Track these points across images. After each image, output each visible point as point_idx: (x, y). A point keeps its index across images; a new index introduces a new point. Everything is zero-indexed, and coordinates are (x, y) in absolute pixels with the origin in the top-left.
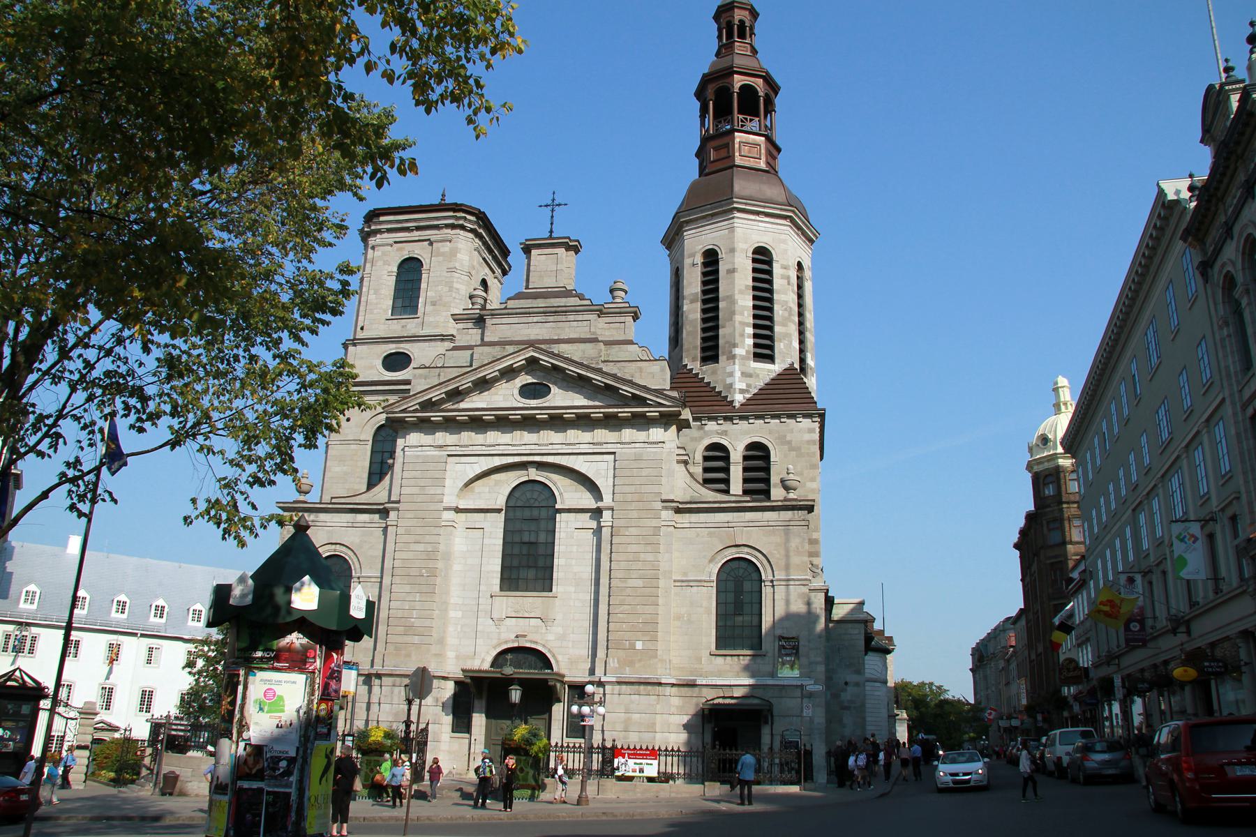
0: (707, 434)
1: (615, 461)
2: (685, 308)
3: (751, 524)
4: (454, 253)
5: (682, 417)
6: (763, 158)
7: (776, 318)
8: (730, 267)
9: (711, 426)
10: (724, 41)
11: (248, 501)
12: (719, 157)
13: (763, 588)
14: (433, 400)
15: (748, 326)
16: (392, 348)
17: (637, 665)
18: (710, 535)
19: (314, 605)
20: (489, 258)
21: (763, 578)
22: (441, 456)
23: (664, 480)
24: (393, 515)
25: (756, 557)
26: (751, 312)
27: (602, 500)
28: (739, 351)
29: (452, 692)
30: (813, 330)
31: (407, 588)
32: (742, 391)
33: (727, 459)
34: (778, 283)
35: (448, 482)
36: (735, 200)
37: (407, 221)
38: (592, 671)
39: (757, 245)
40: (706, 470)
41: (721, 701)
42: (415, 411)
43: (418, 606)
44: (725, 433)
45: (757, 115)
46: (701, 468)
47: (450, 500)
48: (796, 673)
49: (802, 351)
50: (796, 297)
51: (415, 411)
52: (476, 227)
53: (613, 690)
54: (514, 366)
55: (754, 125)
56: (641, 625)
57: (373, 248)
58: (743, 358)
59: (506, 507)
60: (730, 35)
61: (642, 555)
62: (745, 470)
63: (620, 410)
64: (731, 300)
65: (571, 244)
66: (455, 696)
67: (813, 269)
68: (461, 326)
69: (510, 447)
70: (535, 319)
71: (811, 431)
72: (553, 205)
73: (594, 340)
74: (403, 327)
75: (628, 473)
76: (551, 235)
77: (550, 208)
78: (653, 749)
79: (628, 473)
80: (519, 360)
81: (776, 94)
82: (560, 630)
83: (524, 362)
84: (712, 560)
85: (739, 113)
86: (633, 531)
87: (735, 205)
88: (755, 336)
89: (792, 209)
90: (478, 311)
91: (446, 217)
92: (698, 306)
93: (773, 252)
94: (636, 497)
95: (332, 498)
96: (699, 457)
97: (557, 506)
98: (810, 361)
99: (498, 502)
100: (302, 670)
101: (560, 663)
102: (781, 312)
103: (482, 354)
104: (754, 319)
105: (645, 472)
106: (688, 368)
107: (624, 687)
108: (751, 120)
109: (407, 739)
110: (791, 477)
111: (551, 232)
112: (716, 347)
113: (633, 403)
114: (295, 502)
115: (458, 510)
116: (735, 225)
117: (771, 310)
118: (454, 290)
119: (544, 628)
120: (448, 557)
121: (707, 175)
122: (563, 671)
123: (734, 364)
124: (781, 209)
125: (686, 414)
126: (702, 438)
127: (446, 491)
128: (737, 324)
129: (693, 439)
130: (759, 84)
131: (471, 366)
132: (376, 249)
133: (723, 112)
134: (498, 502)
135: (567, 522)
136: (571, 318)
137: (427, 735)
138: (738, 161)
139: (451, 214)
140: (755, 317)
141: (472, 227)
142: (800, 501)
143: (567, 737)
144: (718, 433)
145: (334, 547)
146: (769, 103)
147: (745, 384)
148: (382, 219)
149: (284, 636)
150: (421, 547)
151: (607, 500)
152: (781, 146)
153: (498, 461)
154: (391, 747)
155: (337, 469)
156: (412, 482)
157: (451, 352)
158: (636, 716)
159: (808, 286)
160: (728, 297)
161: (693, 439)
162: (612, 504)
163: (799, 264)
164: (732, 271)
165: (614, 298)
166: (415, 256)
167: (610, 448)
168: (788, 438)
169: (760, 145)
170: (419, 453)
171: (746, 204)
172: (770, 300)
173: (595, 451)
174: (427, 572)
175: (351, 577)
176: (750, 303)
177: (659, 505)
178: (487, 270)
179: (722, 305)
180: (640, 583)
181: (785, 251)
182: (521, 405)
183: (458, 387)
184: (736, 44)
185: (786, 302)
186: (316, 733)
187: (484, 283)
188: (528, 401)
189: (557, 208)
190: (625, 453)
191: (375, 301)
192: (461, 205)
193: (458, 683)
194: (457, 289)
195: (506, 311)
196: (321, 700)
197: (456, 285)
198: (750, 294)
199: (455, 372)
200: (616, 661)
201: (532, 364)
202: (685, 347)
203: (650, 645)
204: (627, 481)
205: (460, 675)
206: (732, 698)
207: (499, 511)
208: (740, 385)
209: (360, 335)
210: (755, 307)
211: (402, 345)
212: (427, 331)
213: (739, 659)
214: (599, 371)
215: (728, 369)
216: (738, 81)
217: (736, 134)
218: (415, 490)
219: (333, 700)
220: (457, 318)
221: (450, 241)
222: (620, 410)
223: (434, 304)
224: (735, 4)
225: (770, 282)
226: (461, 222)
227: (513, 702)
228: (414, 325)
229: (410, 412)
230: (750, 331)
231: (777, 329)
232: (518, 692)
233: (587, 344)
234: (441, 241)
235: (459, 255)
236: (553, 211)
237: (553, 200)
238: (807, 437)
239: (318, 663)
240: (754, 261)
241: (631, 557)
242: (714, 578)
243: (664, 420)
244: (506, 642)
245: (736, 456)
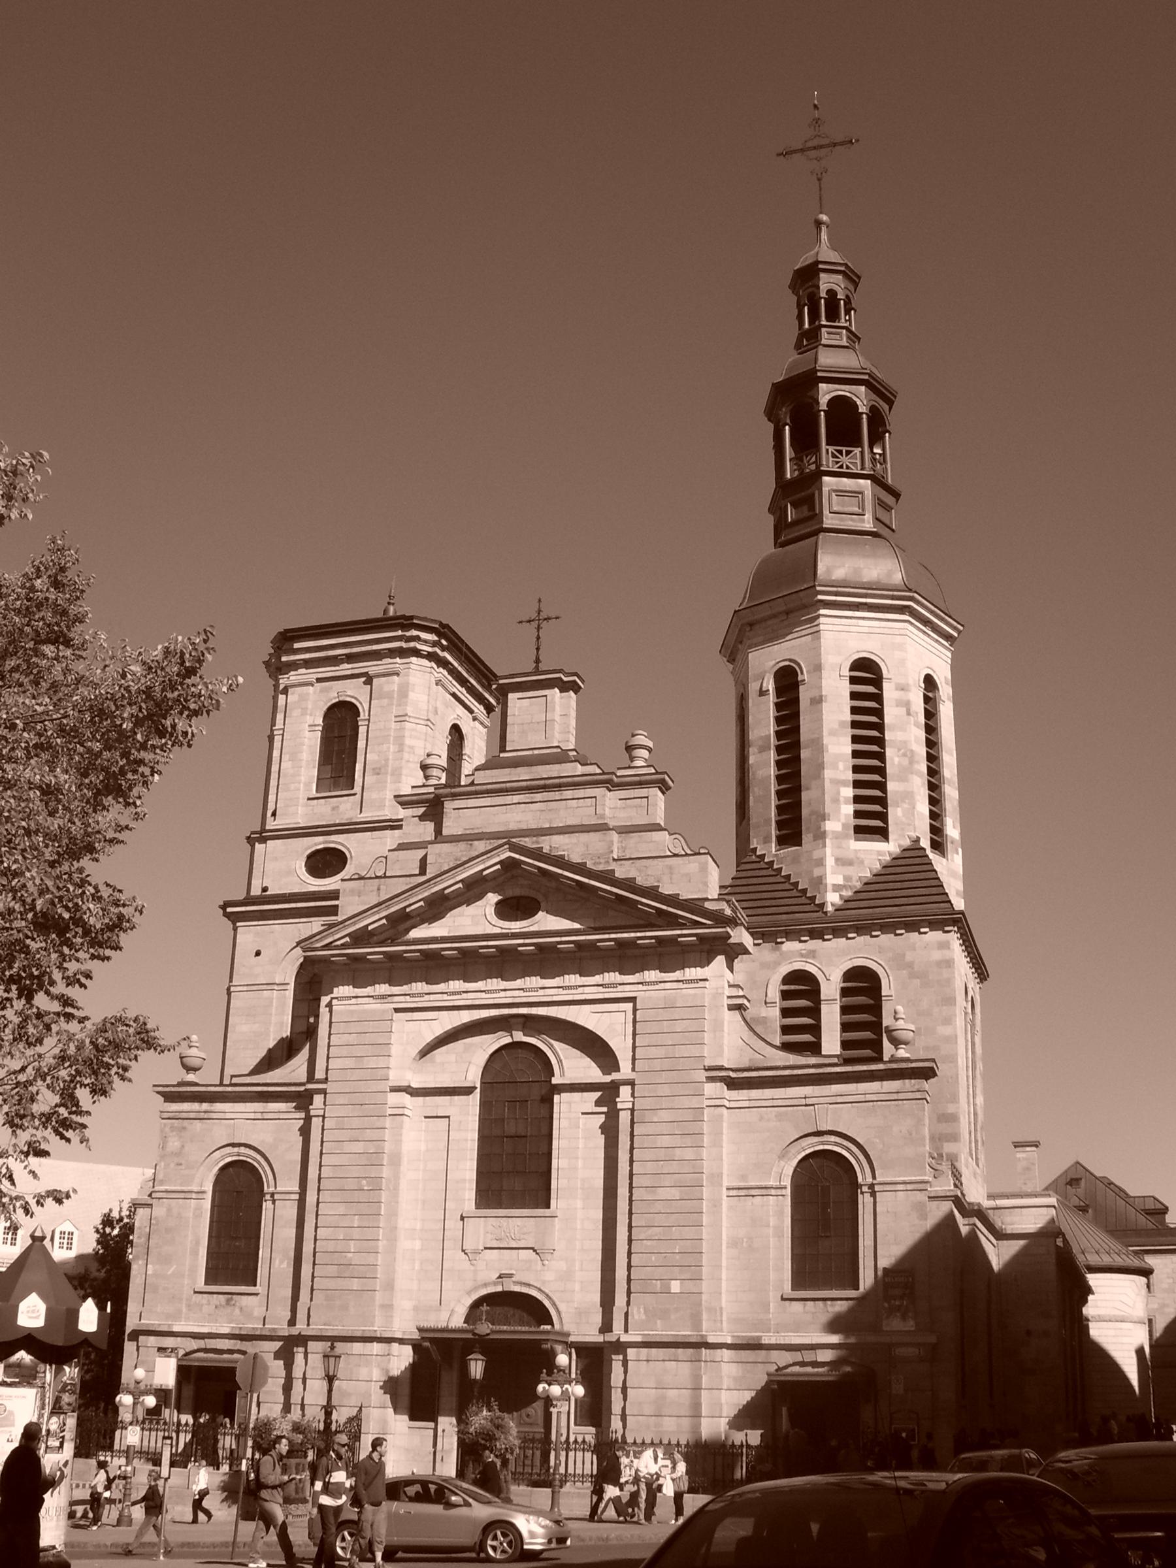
0: (785, 957)
1: (635, 1010)
2: (752, 759)
3: (840, 1099)
4: (404, 692)
5: (732, 941)
6: (869, 516)
7: (890, 770)
8: (814, 693)
9: (790, 946)
10: (807, 326)
11: (28, 1169)
12: (801, 516)
13: (860, 1196)
14: (370, 928)
16: (318, 843)
17: (673, 1317)
18: (778, 1116)
19: (39, 1322)
20: (461, 692)
21: (860, 1180)
22: (384, 1011)
23: (707, 1037)
24: (318, 1100)
25: (848, 1150)
26: (851, 762)
27: (617, 1069)
28: (831, 826)
29: (411, 1361)
30: (956, 779)
31: (341, 1209)
32: (837, 888)
33: (818, 992)
34: (891, 713)
35: (395, 1050)
36: (818, 588)
37: (333, 647)
38: (606, 1327)
40: (786, 1012)
41: (797, 1369)
42: (344, 946)
43: (356, 1233)
44: (812, 954)
45: (858, 443)
46: (778, 1009)
47: (399, 1076)
48: (910, 1325)
49: (934, 816)
50: (922, 734)
51: (344, 946)
52: (437, 650)
53: (638, 1354)
54: (485, 873)
55: (853, 459)
56: (677, 1257)
57: (285, 691)
58: (837, 836)
59: (482, 1083)
60: (814, 315)
61: (678, 1153)
62: (845, 1010)
63: (639, 934)
64: (818, 746)
65: (565, 679)
66: (414, 1368)
67: (956, 683)
68: (410, 812)
69: (483, 995)
70: (516, 799)
71: (945, 946)
72: (539, 620)
73: (603, 828)
74: (333, 809)
75: (654, 1027)
76: (537, 667)
77: (535, 624)
78: (669, 1443)
79: (654, 1027)
80: (490, 865)
81: (890, 403)
82: (562, 1266)
83: (498, 867)
84: (783, 1155)
85: (828, 444)
86: (664, 1115)
87: (820, 597)
88: (857, 799)
89: (911, 594)
90: (432, 790)
91: (389, 639)
92: (772, 755)
94: (667, 1064)
95: (232, 1076)
96: (774, 993)
97: (554, 1081)
98: (952, 830)
99: (470, 1077)
100: (30, 1385)
101: (563, 1315)
102: (896, 760)
103: (439, 855)
104: (854, 772)
105: (679, 1026)
106: (758, 853)
107: (654, 1351)
108: (848, 453)
109: (327, 1432)
110: (901, 1024)
111: (537, 661)
112: (798, 819)
113: (659, 921)
114: (180, 1084)
115: (414, 1092)
116: (822, 627)
117: (881, 756)
118: (406, 749)
119: (540, 1262)
120: (396, 1160)
121: (783, 545)
122: (566, 1328)
123: (824, 846)
124: (893, 598)
125: (740, 935)
126: (777, 964)
127: (393, 1062)
128: (827, 784)
129: (765, 966)
130: (861, 397)
131: (423, 871)
132: (290, 691)
133: (806, 443)
134: (470, 1077)
135: (569, 1103)
136: (568, 794)
137: (359, 1426)
138: (829, 521)
139: (400, 633)
140: (856, 769)
141: (430, 649)
142: (912, 1061)
143: (576, 1424)
144: (802, 956)
145: (236, 1150)
146: (877, 420)
147: (841, 878)
149: (13, 1354)
150: (359, 1147)
151: (625, 1071)
152: (898, 487)
153: (466, 1017)
154: (301, 1444)
155: (244, 1028)
156: (344, 1051)
157: (396, 853)
158: (672, 1393)
159: (946, 712)
160: (813, 741)
161: (765, 966)
162: (632, 1076)
163: (929, 682)
164: (818, 701)
165: (632, 759)
166: (348, 699)
167: (627, 991)
168: (909, 957)
169: (861, 493)
170: (353, 1007)
171: (837, 594)
172: (880, 742)
173: (607, 996)
174: (368, 1184)
175: (262, 1194)
176: (847, 748)
177: (703, 1075)
178: (460, 710)
179: (804, 754)
180: (675, 1193)
181: (903, 662)
182: (498, 931)
183: (405, 908)
184: (824, 330)
185: (905, 742)
186: (47, 1447)
187: (456, 730)
188: (507, 924)
189: (544, 624)
190: (650, 998)
192: (412, 618)
193: (417, 1347)
194: (412, 747)
195: (473, 788)
196: (52, 1413)
197: (408, 741)
198: (849, 732)
199: (401, 885)
200: (642, 1310)
201: (509, 866)
202: (753, 821)
203: (691, 1286)
204: (654, 1039)
205: (416, 1336)
206: (815, 1364)
207: (468, 1091)
208: (833, 877)
209: (271, 824)
210: (856, 754)
211: (333, 838)
212: (367, 815)
213: (825, 1306)
214: (607, 877)
215: (816, 855)
216: (826, 393)
217: (826, 479)
218: (350, 1063)
219: (66, 1413)
220: (404, 802)
221: (398, 674)
222: (639, 934)
223: (377, 772)
224: (820, 266)
225: (879, 713)
226: (412, 644)
227: (473, 1377)
228: (349, 806)
229: (337, 947)
230: (848, 792)
231: (891, 786)
232: (480, 1363)
233: (592, 834)
234: (384, 675)
235: (412, 695)
236: (539, 628)
237: (539, 612)
238: (937, 955)
239: (49, 1377)
240: (853, 680)
241: (661, 1154)
242: (787, 1182)
243: (706, 947)
244: (485, 1285)
245: (831, 988)
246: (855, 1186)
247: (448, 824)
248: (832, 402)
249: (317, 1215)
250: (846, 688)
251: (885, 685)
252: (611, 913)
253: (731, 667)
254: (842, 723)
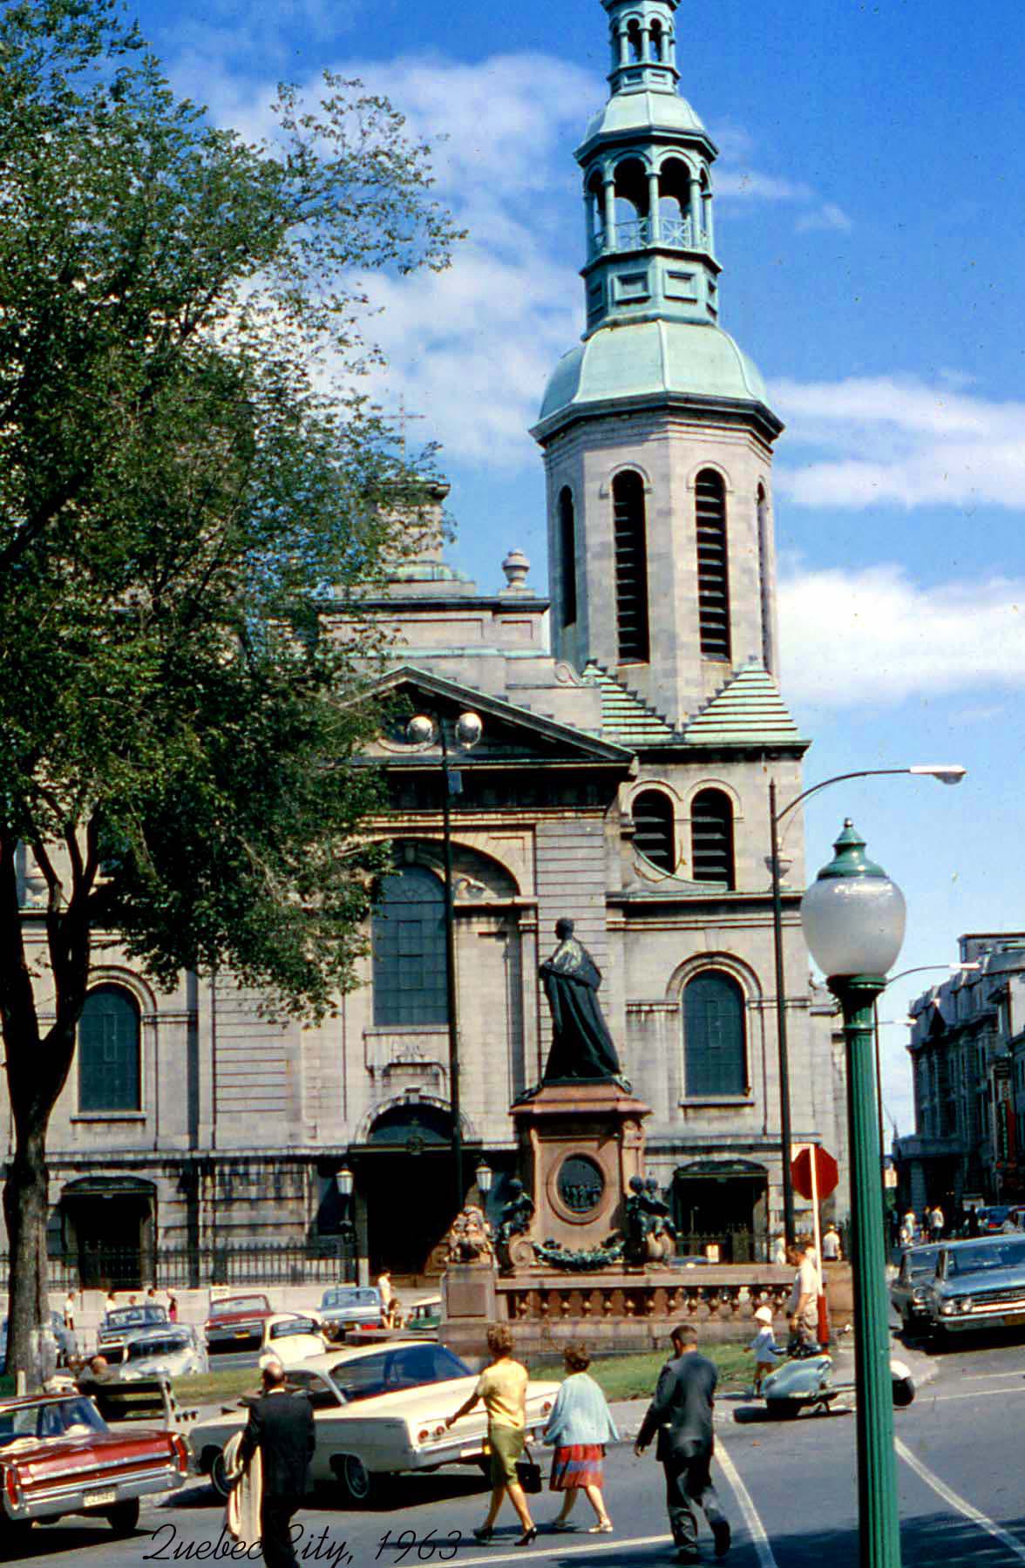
8: (661, 505)
39: (701, 468)
64: (667, 558)
92: (611, 565)
93: (725, 477)
116: (670, 434)
164: (668, 513)
198: (694, 547)
231: (734, 605)
240: (700, 491)
245: (682, 811)
246: (741, 1003)
249: (214, 1038)
250: (691, 499)
251: (729, 499)
253: (542, 450)
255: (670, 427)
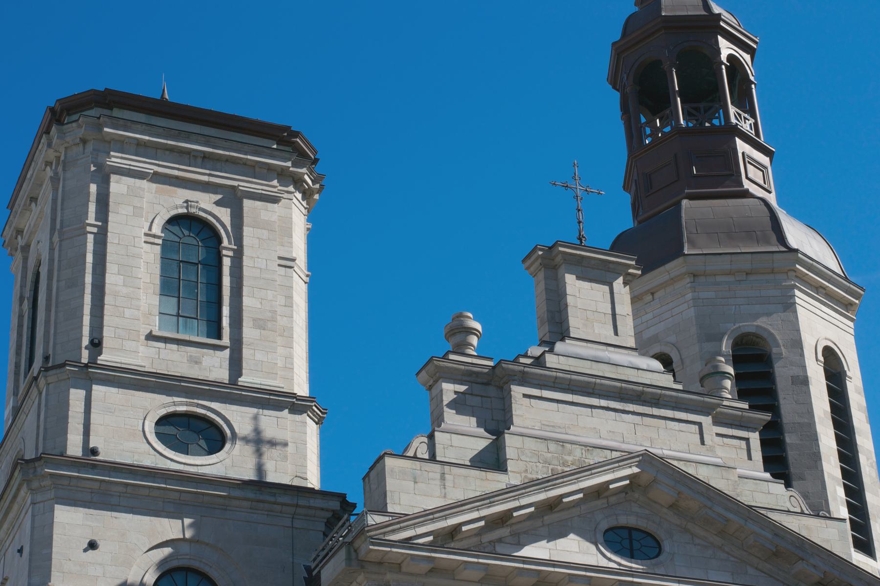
15: (839, 485)
102: (867, 469)
148: (117, 112)
179: (789, 439)
191: (125, 291)
223: (260, 324)
230: (841, 492)
247: (518, 413)
248: (731, 57)
252: (751, 571)
254: (825, 411)
255: (797, 293)
